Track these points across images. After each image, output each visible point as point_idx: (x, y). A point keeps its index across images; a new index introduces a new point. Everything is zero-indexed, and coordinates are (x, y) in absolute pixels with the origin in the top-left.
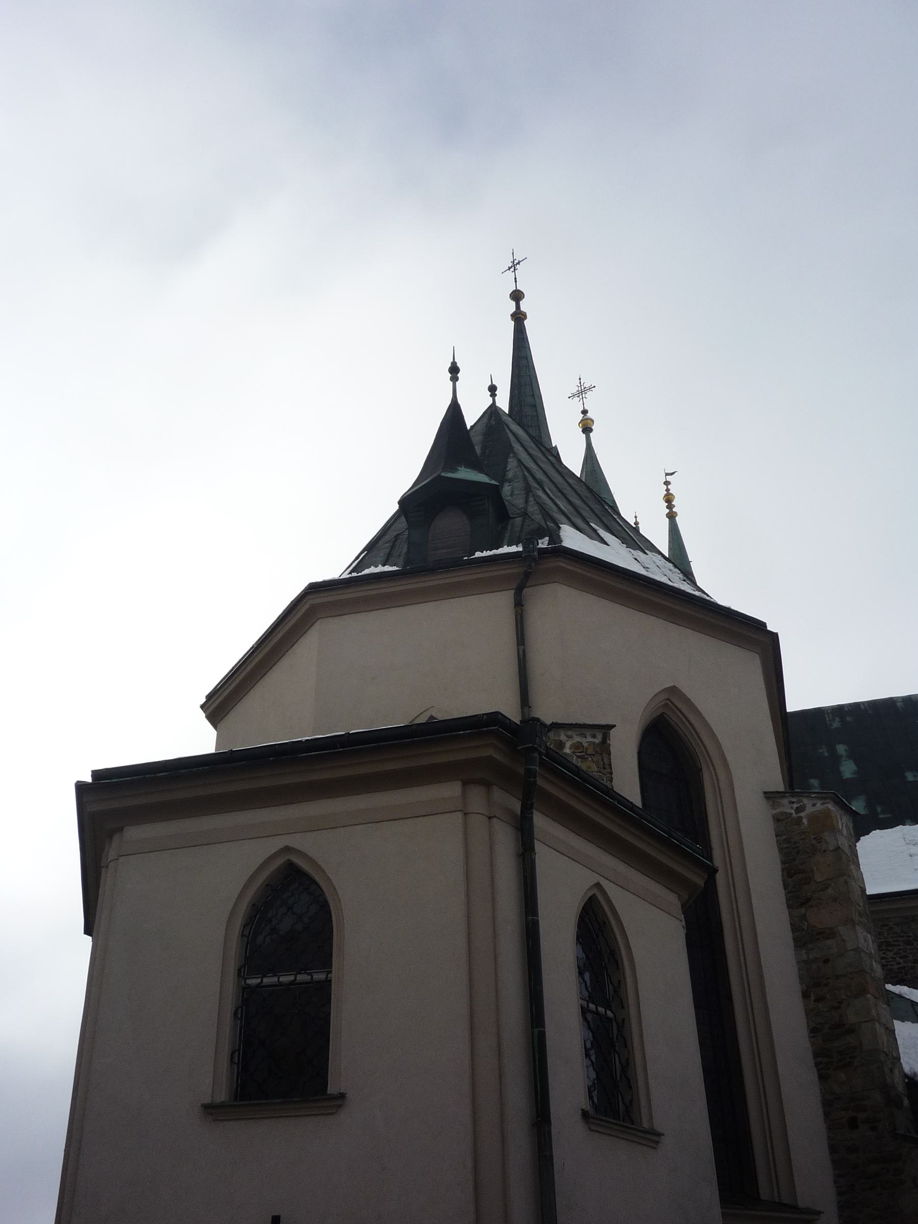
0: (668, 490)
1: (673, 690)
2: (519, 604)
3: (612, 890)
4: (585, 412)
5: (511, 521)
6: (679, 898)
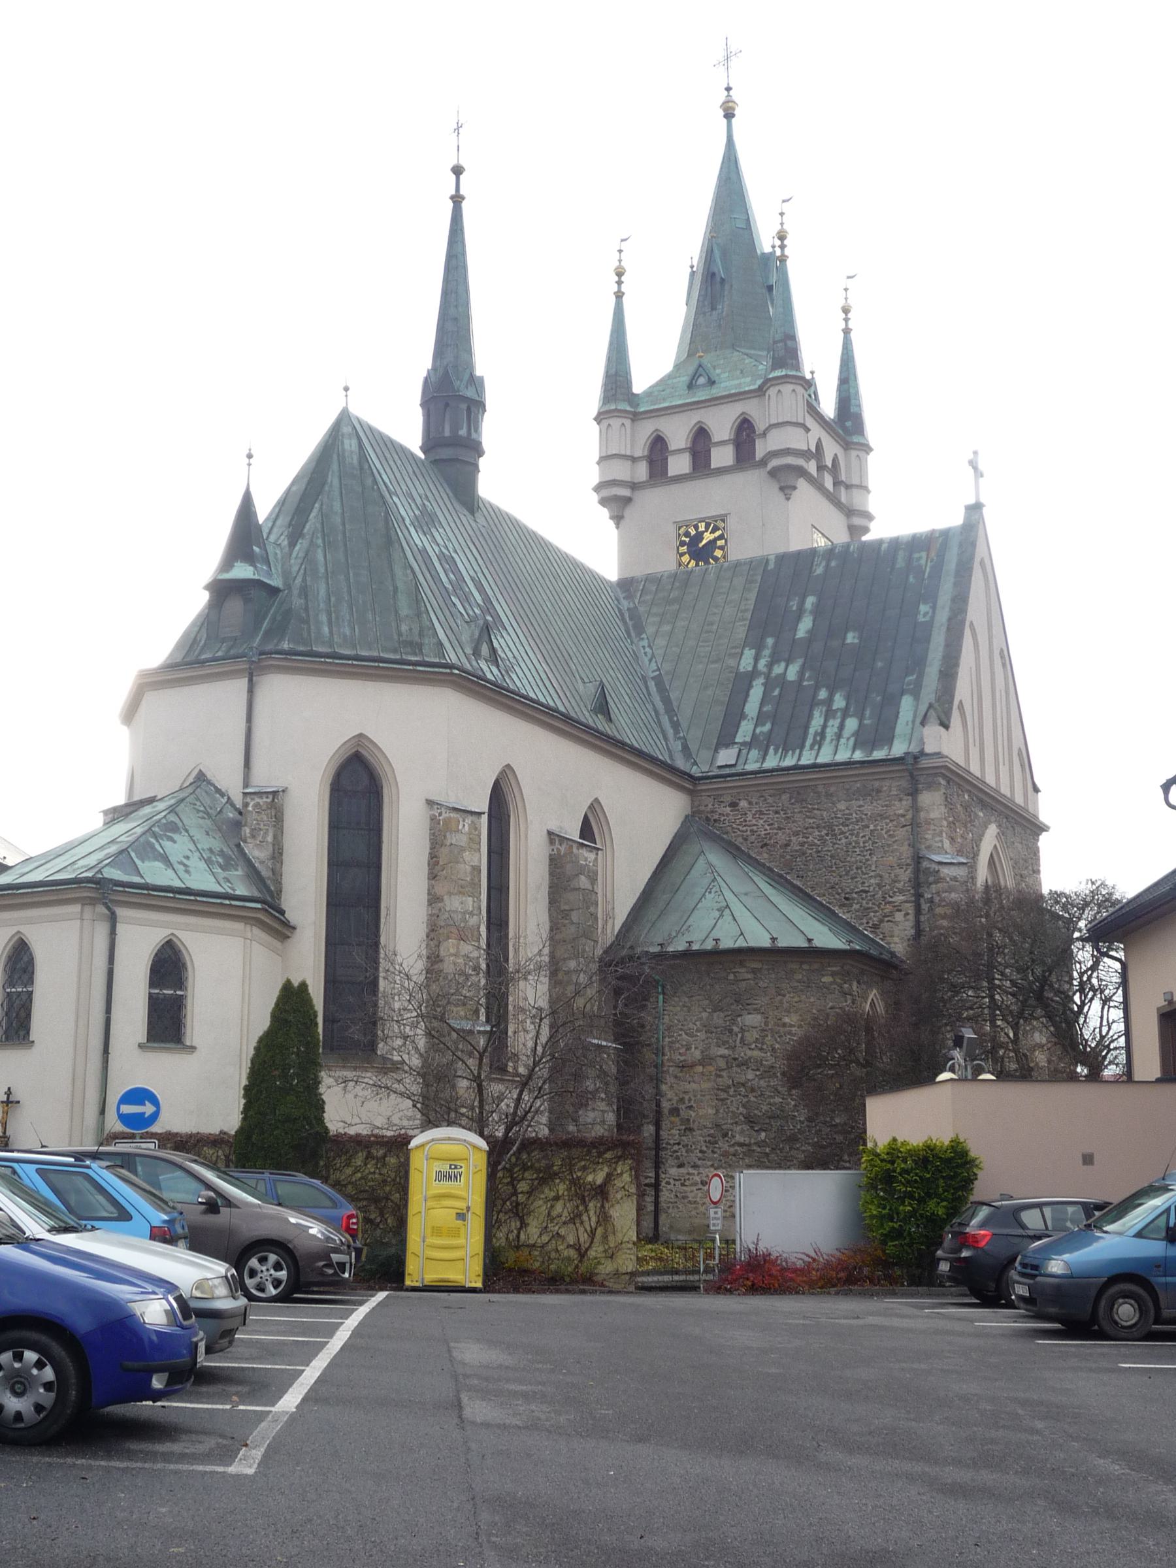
1: (361, 735)
2: (251, 691)
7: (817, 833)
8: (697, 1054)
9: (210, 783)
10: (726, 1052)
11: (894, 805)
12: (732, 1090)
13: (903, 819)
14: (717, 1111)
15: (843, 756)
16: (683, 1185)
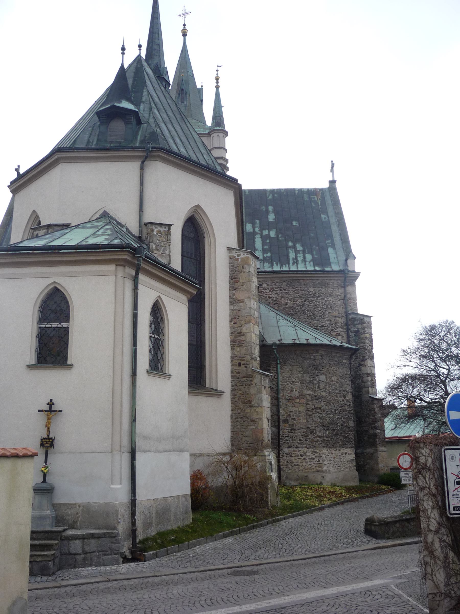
0: (217, 74)
1: (198, 206)
2: (142, 168)
3: (163, 297)
4: (184, 25)
5: (142, 125)
6: (187, 297)
7: (300, 300)
8: (297, 394)
9: (112, 218)
10: (311, 393)
11: (336, 291)
12: (314, 410)
13: (339, 297)
14: (307, 421)
15: (310, 268)
16: (291, 456)
